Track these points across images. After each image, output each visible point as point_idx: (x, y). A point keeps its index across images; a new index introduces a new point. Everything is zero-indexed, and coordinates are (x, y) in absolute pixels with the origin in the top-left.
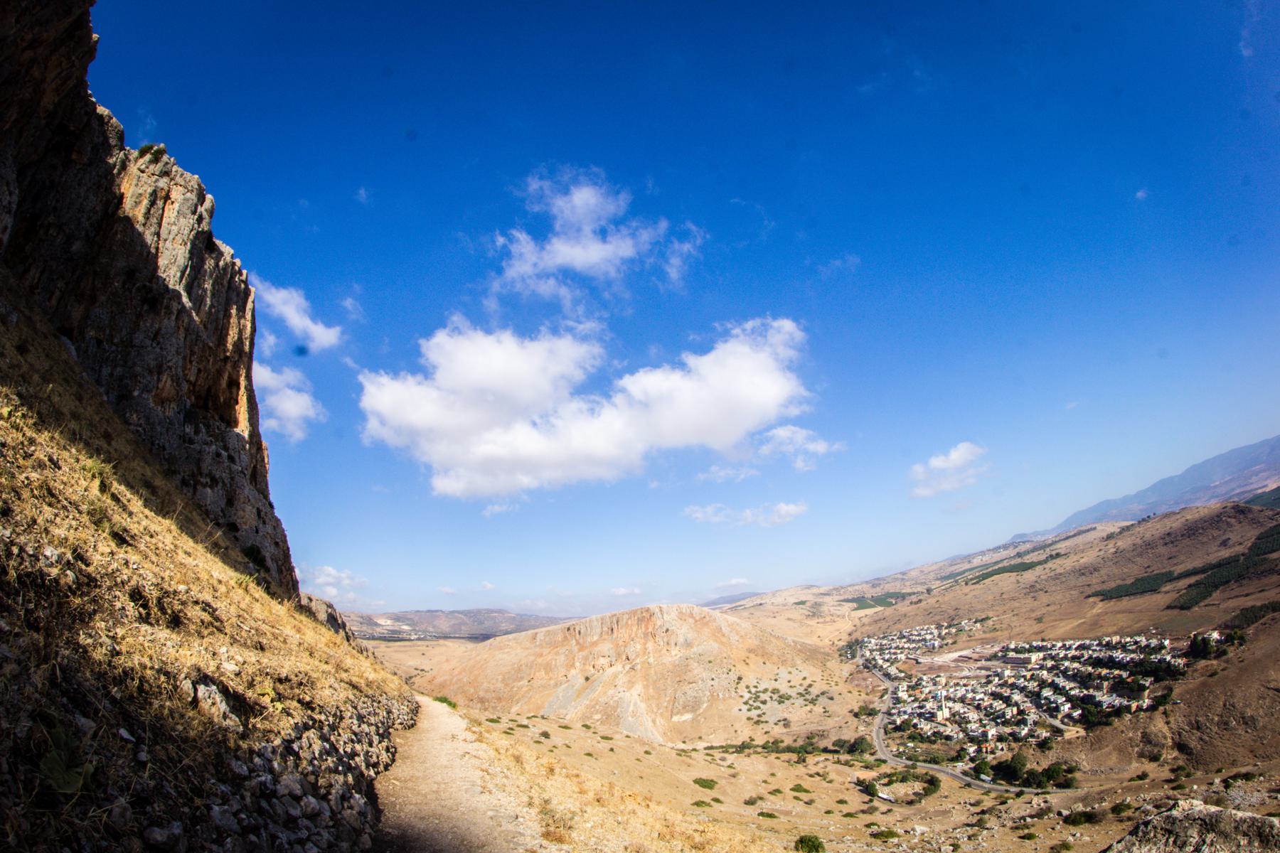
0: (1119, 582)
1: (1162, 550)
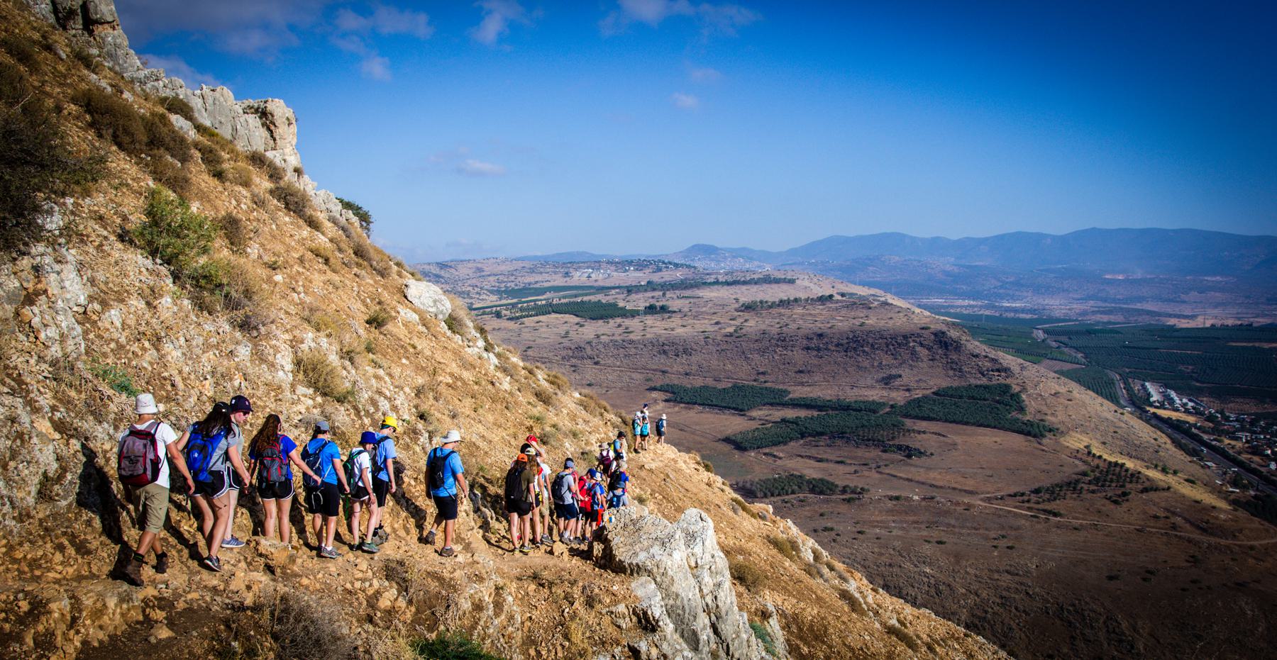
0: (710, 382)
1: (798, 356)
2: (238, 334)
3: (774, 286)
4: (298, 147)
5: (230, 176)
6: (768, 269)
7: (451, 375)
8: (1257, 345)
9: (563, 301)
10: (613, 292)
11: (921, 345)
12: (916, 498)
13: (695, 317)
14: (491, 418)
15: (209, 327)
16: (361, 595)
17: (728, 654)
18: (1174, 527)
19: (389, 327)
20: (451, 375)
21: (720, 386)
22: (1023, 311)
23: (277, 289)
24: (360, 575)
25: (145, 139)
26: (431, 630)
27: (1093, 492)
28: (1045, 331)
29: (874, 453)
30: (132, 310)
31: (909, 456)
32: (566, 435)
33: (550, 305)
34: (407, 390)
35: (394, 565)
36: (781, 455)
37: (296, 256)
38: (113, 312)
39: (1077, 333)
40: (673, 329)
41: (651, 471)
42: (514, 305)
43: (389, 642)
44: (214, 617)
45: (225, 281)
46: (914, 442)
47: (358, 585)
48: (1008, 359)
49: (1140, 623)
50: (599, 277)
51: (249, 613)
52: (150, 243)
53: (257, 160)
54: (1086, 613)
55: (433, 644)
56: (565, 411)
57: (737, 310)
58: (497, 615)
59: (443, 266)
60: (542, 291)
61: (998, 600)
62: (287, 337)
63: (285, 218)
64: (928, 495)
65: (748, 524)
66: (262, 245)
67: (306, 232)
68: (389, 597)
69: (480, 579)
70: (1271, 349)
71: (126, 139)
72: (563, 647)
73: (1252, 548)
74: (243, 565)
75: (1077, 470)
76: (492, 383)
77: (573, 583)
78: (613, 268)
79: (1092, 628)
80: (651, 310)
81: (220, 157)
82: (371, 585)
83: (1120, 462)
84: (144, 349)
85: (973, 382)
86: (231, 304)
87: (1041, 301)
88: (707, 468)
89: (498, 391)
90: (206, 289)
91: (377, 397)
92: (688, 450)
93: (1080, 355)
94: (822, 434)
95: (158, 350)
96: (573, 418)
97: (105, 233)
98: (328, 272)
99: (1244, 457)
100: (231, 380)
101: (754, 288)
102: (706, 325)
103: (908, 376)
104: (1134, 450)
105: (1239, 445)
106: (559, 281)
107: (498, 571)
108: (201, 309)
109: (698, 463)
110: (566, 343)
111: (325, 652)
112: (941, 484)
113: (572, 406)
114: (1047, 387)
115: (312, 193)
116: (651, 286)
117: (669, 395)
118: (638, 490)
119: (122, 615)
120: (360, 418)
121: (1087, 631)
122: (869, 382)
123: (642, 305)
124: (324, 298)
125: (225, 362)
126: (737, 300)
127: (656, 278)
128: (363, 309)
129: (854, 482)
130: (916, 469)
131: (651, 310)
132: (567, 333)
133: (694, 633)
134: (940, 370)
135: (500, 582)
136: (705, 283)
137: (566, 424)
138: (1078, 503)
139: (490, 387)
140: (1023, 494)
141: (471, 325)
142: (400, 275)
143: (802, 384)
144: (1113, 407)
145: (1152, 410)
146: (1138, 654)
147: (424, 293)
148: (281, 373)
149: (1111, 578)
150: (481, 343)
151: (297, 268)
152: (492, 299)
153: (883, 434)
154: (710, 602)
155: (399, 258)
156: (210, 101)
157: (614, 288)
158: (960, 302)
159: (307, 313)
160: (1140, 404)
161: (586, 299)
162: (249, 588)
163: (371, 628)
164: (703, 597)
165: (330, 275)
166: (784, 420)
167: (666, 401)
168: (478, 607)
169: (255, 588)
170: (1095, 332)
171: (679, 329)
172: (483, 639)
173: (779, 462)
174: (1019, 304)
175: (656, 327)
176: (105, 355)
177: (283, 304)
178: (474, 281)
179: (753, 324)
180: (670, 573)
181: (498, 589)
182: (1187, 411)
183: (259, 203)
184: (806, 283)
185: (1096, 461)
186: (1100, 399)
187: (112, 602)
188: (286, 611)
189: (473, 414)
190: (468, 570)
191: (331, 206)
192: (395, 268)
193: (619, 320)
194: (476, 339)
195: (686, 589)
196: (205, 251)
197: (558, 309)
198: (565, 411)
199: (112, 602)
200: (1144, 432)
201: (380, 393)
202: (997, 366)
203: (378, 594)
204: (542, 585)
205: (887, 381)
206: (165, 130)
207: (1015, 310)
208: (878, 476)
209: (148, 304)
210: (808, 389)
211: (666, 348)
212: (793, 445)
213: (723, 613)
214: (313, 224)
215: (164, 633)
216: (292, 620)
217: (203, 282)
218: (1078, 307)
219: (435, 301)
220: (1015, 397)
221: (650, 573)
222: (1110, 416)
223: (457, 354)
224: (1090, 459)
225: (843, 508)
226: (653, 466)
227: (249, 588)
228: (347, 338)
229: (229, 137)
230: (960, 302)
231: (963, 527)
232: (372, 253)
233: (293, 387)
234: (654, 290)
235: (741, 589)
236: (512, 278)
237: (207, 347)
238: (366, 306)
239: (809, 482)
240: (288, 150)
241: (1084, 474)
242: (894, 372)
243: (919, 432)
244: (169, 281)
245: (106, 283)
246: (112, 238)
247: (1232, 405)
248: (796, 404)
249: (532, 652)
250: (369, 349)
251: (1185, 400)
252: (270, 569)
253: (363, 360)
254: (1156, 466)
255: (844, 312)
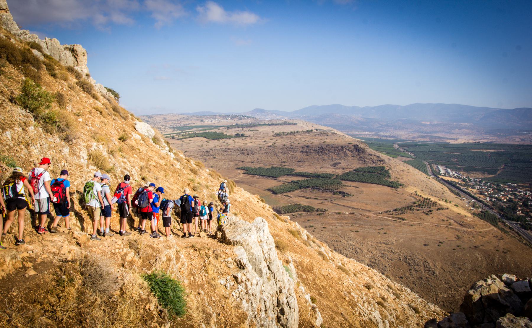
0: (262, 166)
1: (298, 155)
2: (63, 143)
3: (289, 126)
4: (88, 65)
5: (59, 76)
6: (286, 119)
7: (155, 162)
8: (481, 150)
9: (201, 132)
10: (221, 128)
11: (349, 150)
12: (347, 213)
13: (256, 139)
14: (172, 180)
15: (50, 140)
16: (118, 255)
17: (274, 278)
18: (450, 224)
19: (128, 141)
20: (155, 162)
21: (266, 167)
22: (389, 137)
23: (80, 125)
24: (118, 246)
25: (21, 59)
26: (149, 269)
27: (418, 210)
28: (399, 145)
29: (329, 195)
30: (16, 132)
31: (344, 196)
32: (204, 187)
33: (195, 134)
34: (137, 168)
35: (133, 242)
36: (292, 196)
37: (88, 110)
38: (7, 132)
39: (411, 146)
40: (246, 144)
41: (239, 202)
42: (179, 134)
43: (132, 275)
44: (54, 265)
45: (58, 120)
46: (346, 190)
47: (117, 251)
48: (383, 156)
49: (437, 263)
50: (216, 122)
51: (70, 263)
52: (24, 103)
53: (70, 70)
54: (416, 260)
55: (150, 276)
56: (203, 177)
57: (273, 136)
58: (177, 263)
59: (150, 117)
60: (192, 128)
61: (381, 255)
62: (85, 144)
63: (83, 95)
64: (352, 212)
65: (279, 224)
66: (73, 106)
67: (92, 100)
68: (131, 255)
69: (169, 247)
70: (487, 152)
71: (13, 59)
72: (205, 276)
73: (480, 232)
74: (67, 242)
75: (411, 201)
76: (173, 165)
77: (209, 249)
78: (221, 118)
79: (418, 265)
80: (237, 135)
81: (54, 68)
82: (123, 251)
83: (429, 198)
84: (21, 149)
85: (370, 165)
86: (60, 130)
87: (396, 133)
88: (262, 201)
89: (175, 168)
90: (49, 123)
91: (124, 170)
92: (254, 194)
93: (412, 155)
94: (308, 187)
95: (28, 149)
96: (206, 180)
97: (4, 98)
98: (102, 118)
99: (477, 196)
100: (60, 162)
101: (280, 127)
102: (260, 142)
103: (343, 163)
104: (434, 193)
105: (475, 191)
106: (199, 123)
107: (177, 244)
108: (47, 132)
109: (259, 199)
110: (202, 149)
111: (104, 280)
112: (356, 207)
113: (206, 175)
114: (398, 167)
115: (94, 85)
116: (237, 126)
117: (245, 171)
118: (234, 210)
119: (13, 265)
120: (117, 179)
121: (416, 267)
122: (328, 166)
123: (233, 134)
124: (100, 129)
125: (58, 155)
126: (273, 132)
127: (239, 122)
128: (117, 133)
129: (321, 207)
130: (346, 202)
131: (237, 135)
132: (202, 145)
133: (260, 270)
134: (356, 161)
135: (178, 249)
136: (260, 125)
137: (204, 183)
138: (412, 215)
139: (171, 167)
140: (390, 211)
141: (163, 141)
142: (133, 120)
143: (300, 166)
144: (426, 176)
145: (441, 177)
146: (436, 276)
147: (143, 127)
148: (82, 160)
149: (425, 245)
150: (167, 149)
151: (88, 116)
152: (171, 131)
153: (333, 187)
154: (267, 257)
155: (132, 112)
156: (49, 44)
157: (222, 126)
158: (364, 133)
159: (93, 135)
160: (436, 174)
161: (210, 131)
162: (69, 252)
163: (124, 269)
164: (264, 254)
165: (103, 119)
166: (292, 182)
167: (244, 174)
168: (169, 260)
169: (72, 252)
170: (418, 145)
171: (248, 143)
172: (171, 273)
173: (291, 199)
174: (388, 134)
175: (239, 143)
176: (4, 151)
177: (83, 131)
178: (163, 124)
179: (280, 142)
180: (250, 244)
181: (177, 252)
182: (455, 177)
183: (71, 88)
184: (302, 125)
185: (419, 198)
186: (420, 173)
187: (8, 259)
188: (87, 262)
189: (164, 178)
190: (165, 244)
191: (102, 91)
192: (130, 117)
193: (224, 140)
194: (165, 147)
195: (257, 251)
196: (48, 107)
197: (198, 135)
198: (203, 177)
199: (8, 259)
200: (438, 186)
201: (125, 169)
202: (379, 159)
203: (126, 255)
204: (196, 250)
205: (335, 165)
206: (30, 55)
207: (386, 136)
208: (331, 204)
209: (23, 129)
210: (302, 168)
211: (244, 151)
212: (297, 192)
213: (272, 261)
214: (95, 97)
215: (32, 273)
216: (89, 266)
217: (48, 120)
218: (412, 135)
219: (148, 131)
220: (387, 172)
221: (242, 244)
222: (424, 179)
223: (157, 153)
224: (417, 197)
225: (317, 218)
226: (240, 200)
227: (69, 252)
228: (111, 145)
229: (58, 60)
230: (364, 133)
231: (366, 225)
232: (121, 110)
233: (87, 165)
234: (239, 127)
235: (279, 251)
236: (179, 122)
237: (50, 148)
238: (118, 132)
239: (303, 207)
240: (83, 66)
241: (415, 203)
242: (337, 161)
243: (348, 186)
244: (33, 119)
245: (4, 120)
246: (7, 101)
247: (472, 175)
248: (298, 175)
249: (192, 279)
250: (120, 151)
251: (454, 173)
252: (78, 244)
253: (117, 154)
254: (443, 200)
255: (317, 137)
